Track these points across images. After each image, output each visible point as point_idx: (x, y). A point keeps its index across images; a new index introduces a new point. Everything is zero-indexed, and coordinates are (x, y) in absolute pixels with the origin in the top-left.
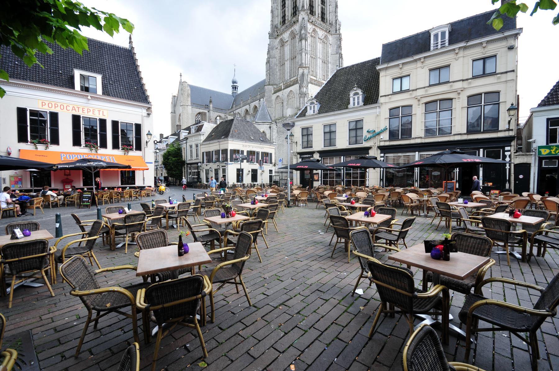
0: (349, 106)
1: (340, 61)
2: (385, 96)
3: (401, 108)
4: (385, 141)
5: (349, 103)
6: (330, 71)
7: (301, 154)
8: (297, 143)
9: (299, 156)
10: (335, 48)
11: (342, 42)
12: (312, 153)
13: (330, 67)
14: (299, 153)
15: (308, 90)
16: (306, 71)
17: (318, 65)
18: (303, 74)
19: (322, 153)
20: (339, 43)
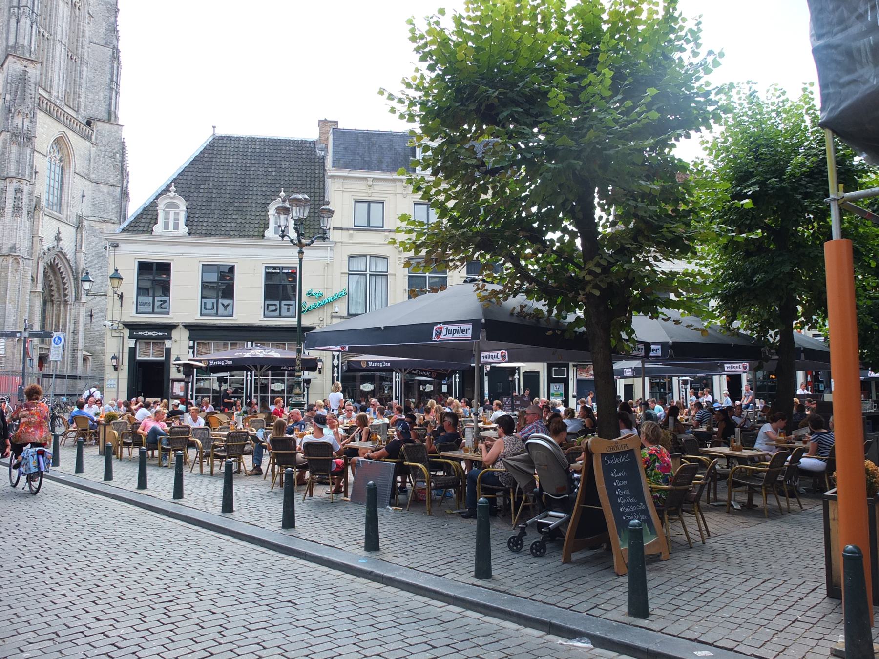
0: (266, 233)
1: (113, 67)
2: (342, 229)
3: (368, 257)
4: (341, 317)
5: (266, 226)
6: (84, 86)
7: (132, 327)
8: (121, 297)
9: (127, 332)
10: (103, 30)
11: (121, 17)
12: (168, 328)
13: (85, 73)
14: (127, 325)
15: (34, 127)
16: (33, 72)
17: (57, 59)
18: (23, 79)
19: (198, 332)
20: (113, 19)
